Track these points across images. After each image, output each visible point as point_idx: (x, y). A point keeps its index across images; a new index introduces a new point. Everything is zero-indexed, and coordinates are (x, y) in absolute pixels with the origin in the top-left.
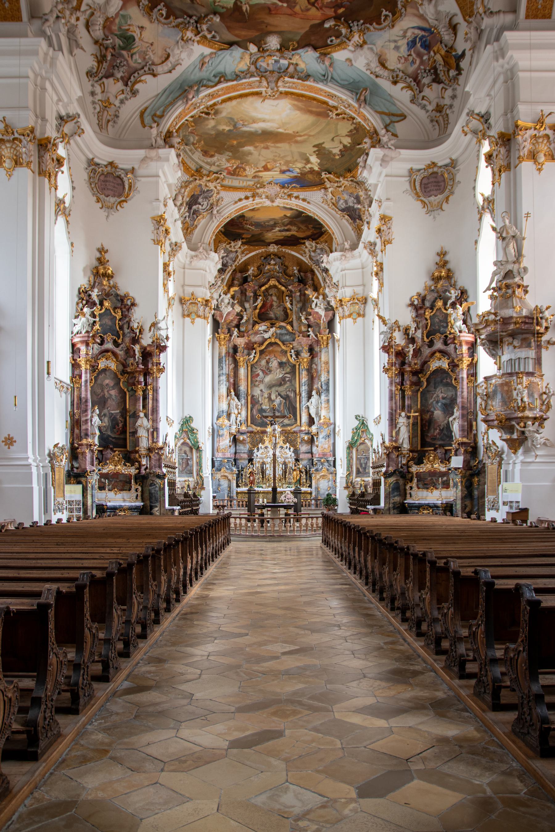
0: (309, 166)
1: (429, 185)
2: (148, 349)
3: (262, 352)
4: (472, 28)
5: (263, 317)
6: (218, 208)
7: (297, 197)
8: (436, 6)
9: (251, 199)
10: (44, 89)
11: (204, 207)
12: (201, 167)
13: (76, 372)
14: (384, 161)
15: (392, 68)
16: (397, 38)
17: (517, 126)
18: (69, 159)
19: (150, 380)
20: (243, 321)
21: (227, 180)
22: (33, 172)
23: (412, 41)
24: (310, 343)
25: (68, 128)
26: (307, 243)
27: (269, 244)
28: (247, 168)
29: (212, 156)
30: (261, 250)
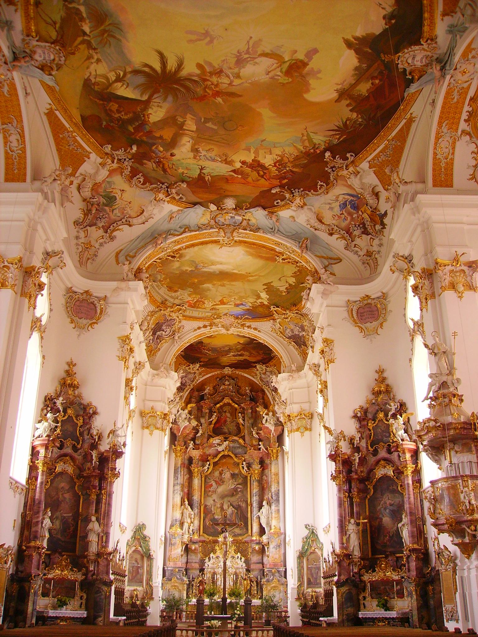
0: (260, 300)
1: (365, 314)
2: (105, 454)
3: (215, 464)
4: (391, 193)
5: (217, 431)
6: (179, 335)
7: (249, 327)
8: (361, 179)
9: (209, 328)
10: (35, 230)
11: (167, 333)
12: (166, 300)
13: (33, 474)
14: (325, 294)
15: (328, 224)
16: (331, 202)
17: (437, 263)
18: (50, 286)
19: (104, 485)
20: (199, 435)
21: (188, 311)
22: (16, 293)
23: (343, 204)
24: (260, 455)
25: (52, 262)
26: (258, 367)
27: (224, 367)
28: (206, 302)
29: (176, 291)
30: (217, 372)
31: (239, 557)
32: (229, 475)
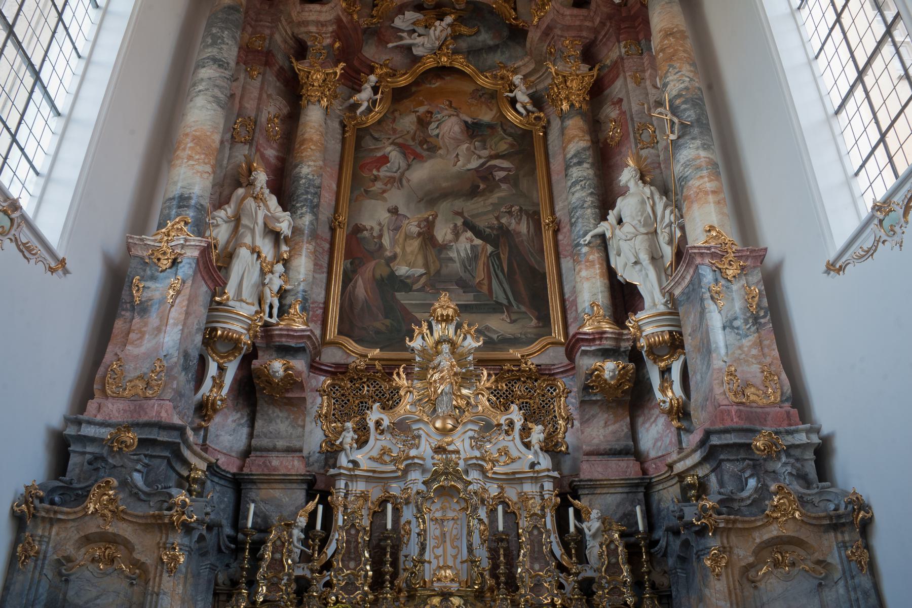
31: (518, 425)
32: (457, 129)
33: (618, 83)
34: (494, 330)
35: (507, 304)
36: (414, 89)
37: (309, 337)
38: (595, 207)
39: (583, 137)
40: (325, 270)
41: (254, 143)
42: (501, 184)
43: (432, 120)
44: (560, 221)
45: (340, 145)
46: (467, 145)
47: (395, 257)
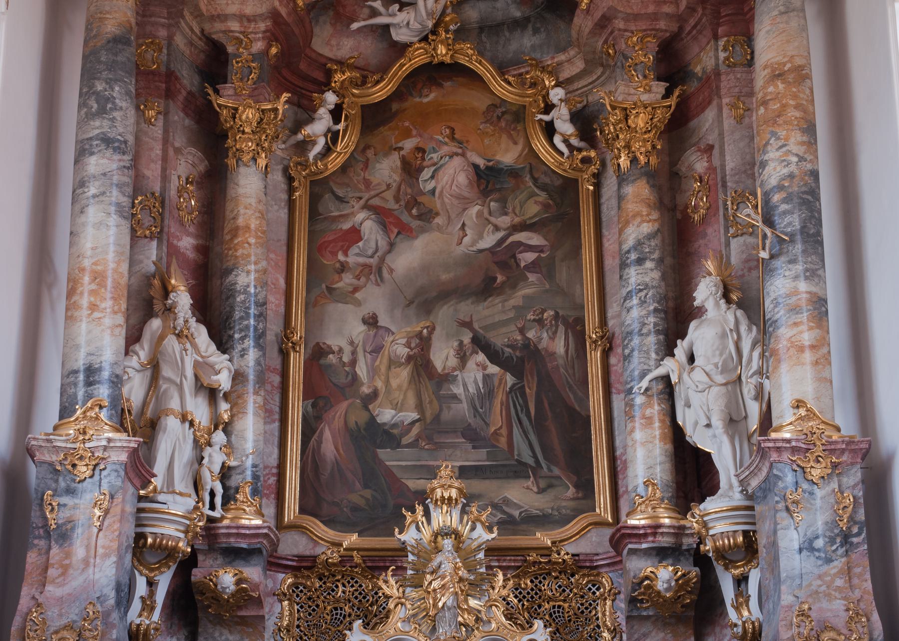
32: (462, 179)
33: (710, 115)
34: (515, 504)
35: (533, 465)
36: (395, 106)
37: (266, 536)
38: (658, 332)
39: (648, 215)
40: (277, 416)
41: (165, 237)
42: (529, 275)
43: (425, 164)
44: (613, 335)
45: (286, 211)
46: (478, 208)
47: (375, 394)
